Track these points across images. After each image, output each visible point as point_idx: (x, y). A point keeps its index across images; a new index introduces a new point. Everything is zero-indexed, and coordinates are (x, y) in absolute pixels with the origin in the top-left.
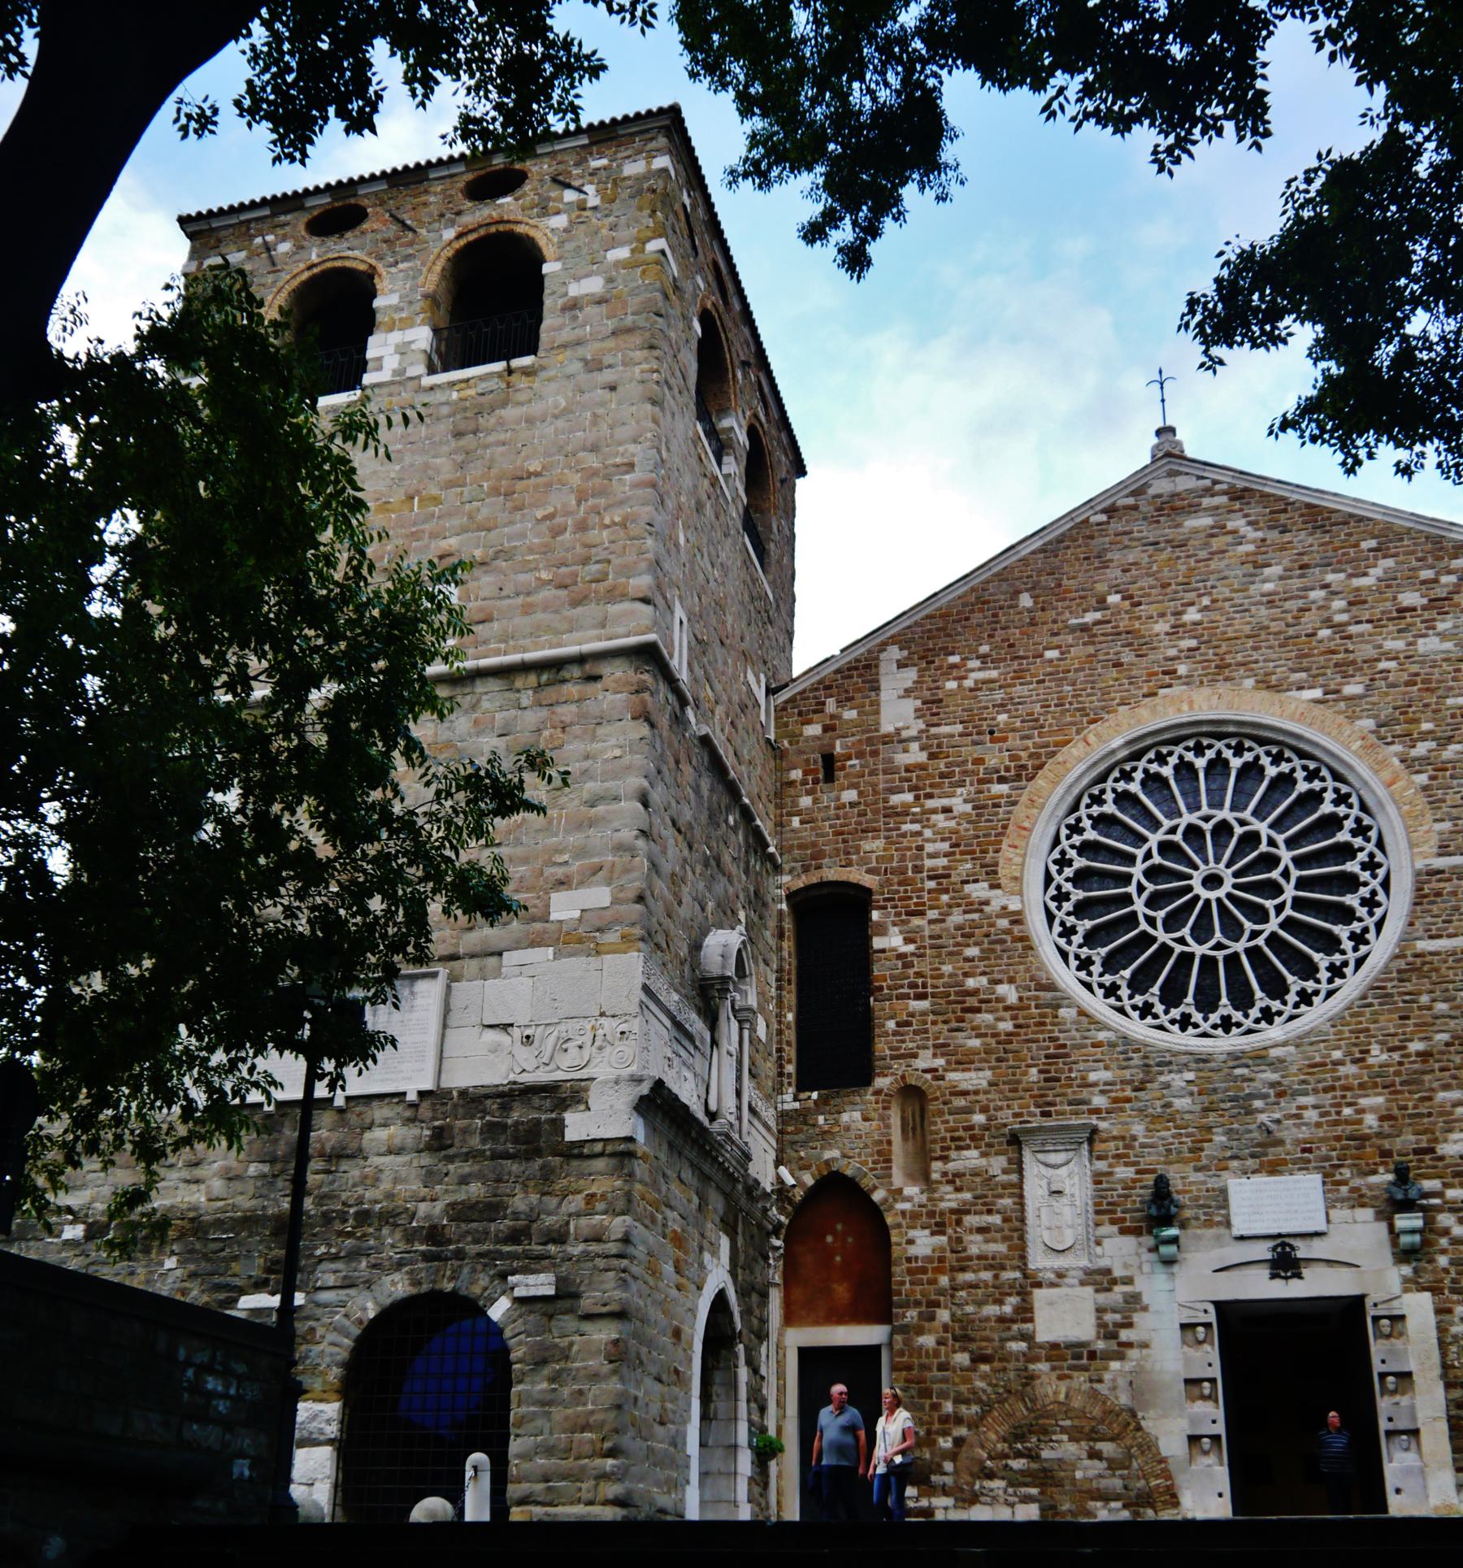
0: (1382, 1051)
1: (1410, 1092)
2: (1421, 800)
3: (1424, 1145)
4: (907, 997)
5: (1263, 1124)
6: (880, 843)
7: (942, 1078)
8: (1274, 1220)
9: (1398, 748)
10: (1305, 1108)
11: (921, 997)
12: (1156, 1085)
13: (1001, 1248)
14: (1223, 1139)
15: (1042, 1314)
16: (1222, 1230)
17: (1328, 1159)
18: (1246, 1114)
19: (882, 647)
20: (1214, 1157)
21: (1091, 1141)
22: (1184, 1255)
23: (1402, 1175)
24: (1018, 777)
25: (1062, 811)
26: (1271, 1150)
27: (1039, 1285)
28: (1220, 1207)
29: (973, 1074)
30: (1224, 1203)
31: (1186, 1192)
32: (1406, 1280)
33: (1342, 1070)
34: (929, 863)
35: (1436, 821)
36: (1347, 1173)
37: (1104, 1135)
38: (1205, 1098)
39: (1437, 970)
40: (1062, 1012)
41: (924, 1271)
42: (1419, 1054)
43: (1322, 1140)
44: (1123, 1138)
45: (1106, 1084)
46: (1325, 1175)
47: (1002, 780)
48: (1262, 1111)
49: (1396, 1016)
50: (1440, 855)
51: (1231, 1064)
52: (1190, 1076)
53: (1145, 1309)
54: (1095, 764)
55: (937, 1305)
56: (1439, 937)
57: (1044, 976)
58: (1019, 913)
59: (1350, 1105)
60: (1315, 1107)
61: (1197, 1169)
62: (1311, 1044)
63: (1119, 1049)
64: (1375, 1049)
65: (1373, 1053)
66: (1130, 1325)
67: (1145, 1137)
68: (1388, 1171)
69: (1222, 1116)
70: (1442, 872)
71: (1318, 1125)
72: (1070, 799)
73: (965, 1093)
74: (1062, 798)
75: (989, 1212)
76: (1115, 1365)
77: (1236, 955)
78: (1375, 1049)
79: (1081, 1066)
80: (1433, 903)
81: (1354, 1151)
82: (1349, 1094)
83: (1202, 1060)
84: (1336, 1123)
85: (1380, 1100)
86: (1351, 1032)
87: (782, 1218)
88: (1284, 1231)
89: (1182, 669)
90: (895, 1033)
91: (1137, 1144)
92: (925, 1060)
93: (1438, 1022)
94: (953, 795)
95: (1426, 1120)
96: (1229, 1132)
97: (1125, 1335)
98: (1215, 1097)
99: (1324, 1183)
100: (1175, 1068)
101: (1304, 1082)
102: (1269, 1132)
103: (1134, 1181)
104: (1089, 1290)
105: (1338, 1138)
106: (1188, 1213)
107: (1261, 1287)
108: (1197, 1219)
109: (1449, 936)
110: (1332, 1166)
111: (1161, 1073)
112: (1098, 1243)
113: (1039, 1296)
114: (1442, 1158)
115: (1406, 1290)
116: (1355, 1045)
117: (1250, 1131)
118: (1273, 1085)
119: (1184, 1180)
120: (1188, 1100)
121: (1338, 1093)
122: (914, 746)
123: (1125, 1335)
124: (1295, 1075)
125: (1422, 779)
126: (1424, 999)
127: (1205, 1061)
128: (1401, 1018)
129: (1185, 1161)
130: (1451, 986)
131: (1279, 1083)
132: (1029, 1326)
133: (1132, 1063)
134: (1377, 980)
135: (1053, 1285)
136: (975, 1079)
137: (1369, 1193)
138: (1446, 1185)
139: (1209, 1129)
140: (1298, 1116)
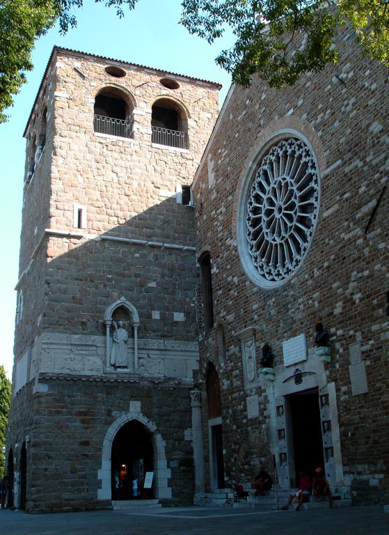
4: (217, 290)
6: (210, 233)
7: (225, 319)
9: (313, 122)
11: (220, 289)
12: (267, 307)
13: (239, 383)
15: (249, 407)
19: (207, 156)
21: (255, 334)
22: (277, 377)
23: (319, 328)
26: (294, 326)
27: (247, 396)
29: (231, 316)
32: (328, 377)
34: (220, 235)
35: (325, 151)
36: (311, 330)
41: (225, 395)
43: (305, 317)
47: (230, 194)
50: (327, 168)
52: (273, 300)
53: (268, 402)
55: (229, 408)
56: (329, 208)
58: (236, 246)
59: (311, 298)
61: (278, 339)
66: (265, 409)
70: (328, 175)
71: (303, 311)
72: (245, 193)
73: (230, 323)
74: (243, 194)
75: (237, 369)
76: (263, 426)
83: (276, 291)
84: (308, 308)
87: (201, 381)
88: (295, 362)
89: (262, 122)
90: (217, 305)
92: (223, 313)
94: (221, 207)
97: (266, 413)
99: (306, 337)
101: (299, 292)
104: (257, 396)
105: (309, 315)
106: (276, 359)
107: (294, 388)
112: (258, 376)
113: (248, 399)
114: (335, 316)
115: (328, 382)
116: (310, 270)
119: (274, 344)
122: (214, 191)
123: (266, 413)
125: (320, 133)
127: (277, 291)
128: (322, 252)
130: (333, 231)
132: (246, 413)
135: (250, 396)
136: (230, 318)
138: (337, 329)
140: (298, 308)
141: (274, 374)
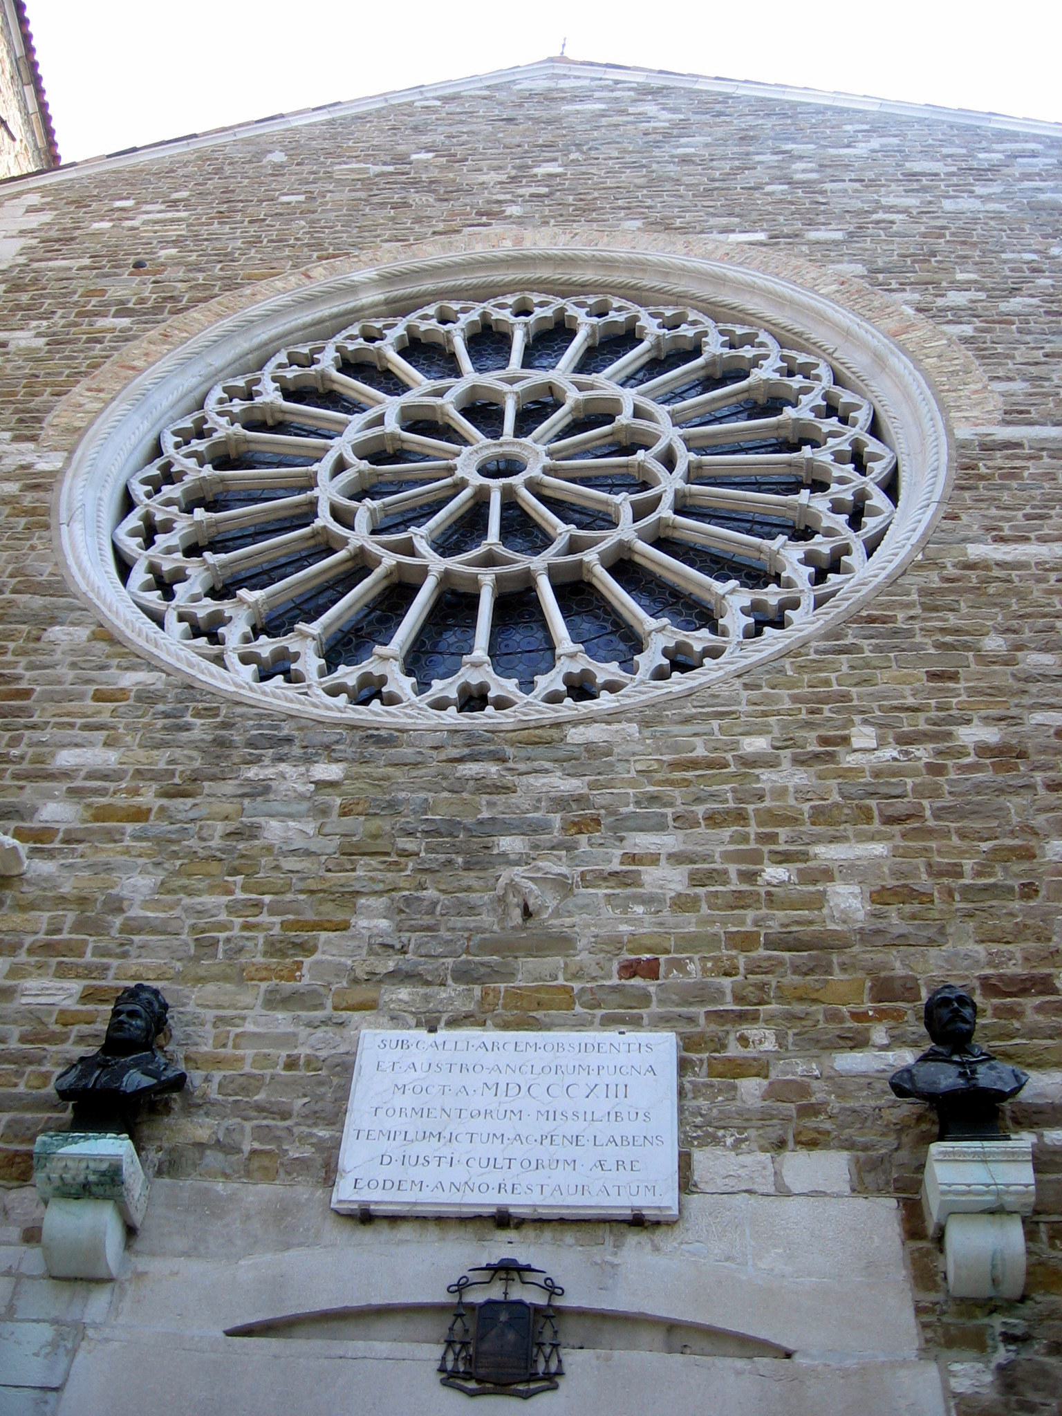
0: (882, 743)
1: (963, 836)
2: (964, 355)
3: (1015, 969)
5: (512, 886)
8: (492, 1163)
10: (654, 860)
12: (229, 787)
14: (384, 924)
16: (304, 1191)
17: (702, 994)
18: (468, 867)
20: (339, 970)
22: (142, 1263)
24: (157, 309)
25: (219, 359)
28: (315, 1117)
30: (335, 1116)
31: (218, 1062)
33: (767, 778)
37: (31, 892)
38: (357, 825)
39: (1022, 596)
40: (55, 632)
42: (983, 750)
43: (689, 943)
44: (83, 901)
45: (91, 776)
46: (688, 1043)
47: (123, 312)
48: (517, 863)
49: (921, 673)
51: (455, 753)
54: (311, 301)
56: (1026, 539)
57: (49, 570)
59: (784, 858)
60: (677, 858)
61: (275, 1001)
62: (687, 720)
63: (161, 707)
64: (863, 736)
65: (856, 743)
67: (146, 904)
68: (897, 1041)
69: (396, 867)
70: (1019, 445)
71: (683, 903)
72: (243, 344)
77: (528, 579)
78: (863, 736)
79: (44, 736)
80: (1003, 487)
81: (792, 979)
82: (783, 832)
84: (740, 901)
85: (879, 849)
86: (795, 699)
88: (519, 1201)
91: (118, 921)
93: (1033, 688)
95: (1016, 905)
96: (401, 910)
98: (384, 824)
100: (296, 751)
101: (654, 799)
102: (527, 913)
103: (67, 1019)
105: (745, 941)
106: (200, 1128)
108: (226, 1147)
109: (1043, 540)
110: (719, 1016)
111: (257, 760)
117: (472, 910)
118: (560, 803)
120: (310, 827)
121: (753, 829)
124: (632, 783)
126: (994, 643)
129: (242, 977)
131: (580, 799)
133: (184, 736)
134: (867, 605)
137: (835, 1104)
139: (349, 897)
141: (131, 1231)
